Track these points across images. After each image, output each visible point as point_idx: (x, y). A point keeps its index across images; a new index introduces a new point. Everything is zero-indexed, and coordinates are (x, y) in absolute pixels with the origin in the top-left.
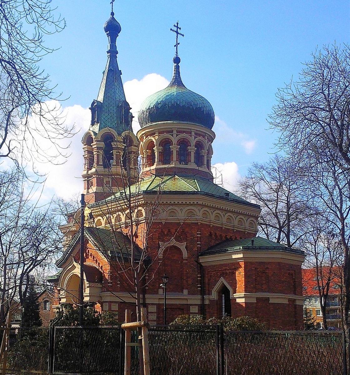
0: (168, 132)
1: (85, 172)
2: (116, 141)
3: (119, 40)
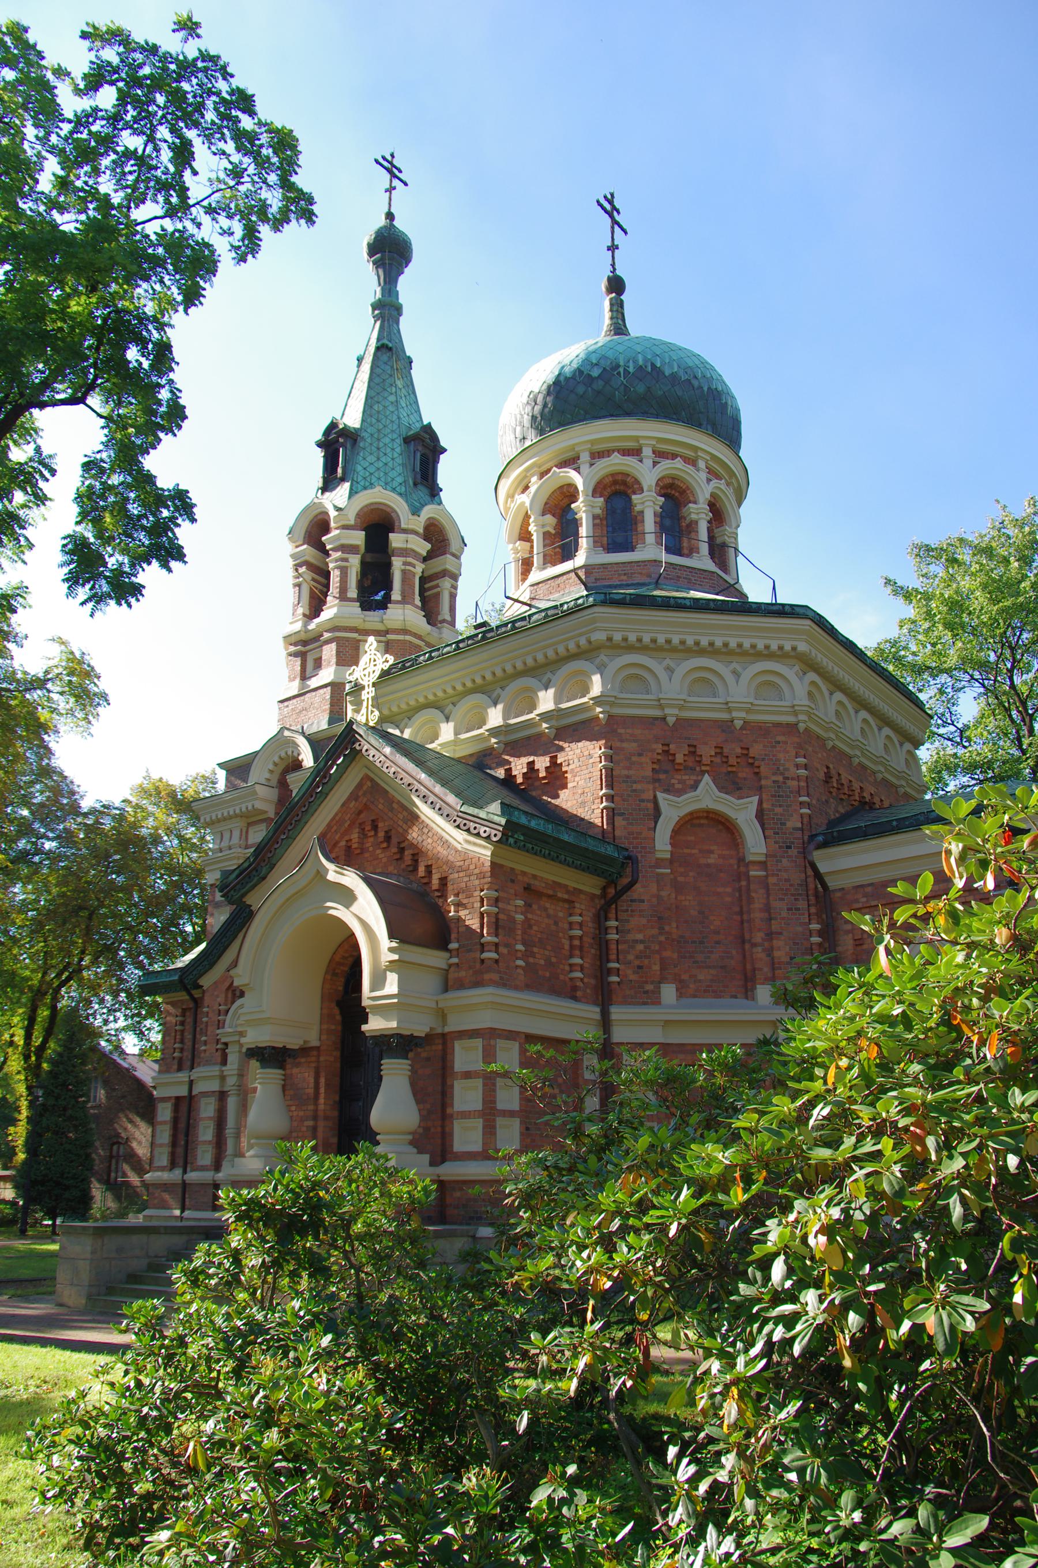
0: (626, 452)
1: (298, 626)
2: (405, 531)
3: (406, 285)
